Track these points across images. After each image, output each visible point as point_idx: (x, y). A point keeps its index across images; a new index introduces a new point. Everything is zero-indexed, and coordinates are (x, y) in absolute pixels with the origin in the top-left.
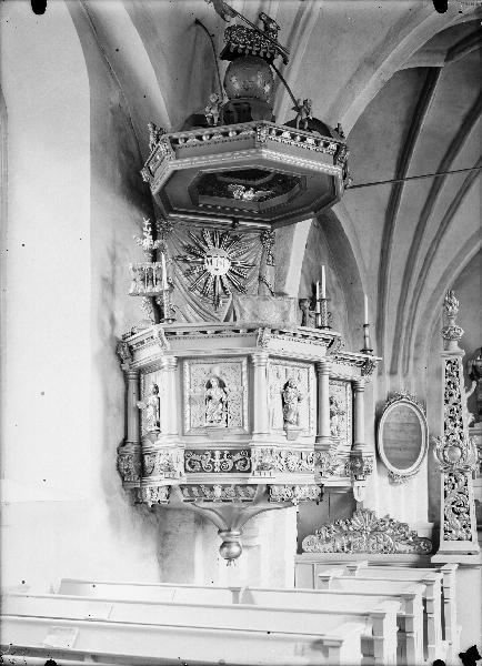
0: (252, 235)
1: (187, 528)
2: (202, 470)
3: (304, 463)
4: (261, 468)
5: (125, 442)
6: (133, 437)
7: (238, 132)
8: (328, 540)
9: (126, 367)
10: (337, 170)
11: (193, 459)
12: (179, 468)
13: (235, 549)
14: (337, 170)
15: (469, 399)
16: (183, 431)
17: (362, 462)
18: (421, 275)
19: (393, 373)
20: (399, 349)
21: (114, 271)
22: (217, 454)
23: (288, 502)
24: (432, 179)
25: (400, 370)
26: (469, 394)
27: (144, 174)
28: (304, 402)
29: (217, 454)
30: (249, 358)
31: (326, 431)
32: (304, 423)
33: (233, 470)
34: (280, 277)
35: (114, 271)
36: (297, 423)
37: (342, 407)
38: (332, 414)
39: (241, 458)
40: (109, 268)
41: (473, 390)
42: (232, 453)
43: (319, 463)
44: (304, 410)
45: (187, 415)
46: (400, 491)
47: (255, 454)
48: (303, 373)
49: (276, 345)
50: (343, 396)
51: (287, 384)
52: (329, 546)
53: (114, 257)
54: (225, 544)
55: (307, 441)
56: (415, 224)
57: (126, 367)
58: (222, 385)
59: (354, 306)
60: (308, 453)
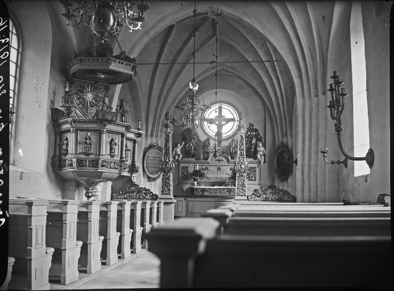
0: (102, 87)
1: (73, 188)
2: (82, 166)
3: (116, 166)
4: (103, 166)
5: (54, 156)
6: (57, 154)
7: (102, 60)
8: (122, 195)
9: (56, 130)
10: (132, 73)
11: (80, 163)
12: (75, 165)
13: (90, 194)
14: (132, 73)
15: (181, 148)
16: (77, 151)
17: (135, 167)
18: (165, 98)
19: (152, 136)
20: (154, 127)
21: (54, 97)
22: (88, 161)
23: (108, 179)
24: (169, 65)
25: (155, 134)
26: (181, 146)
27: (68, 67)
28: (117, 146)
29: (88, 161)
30: (100, 131)
31: (124, 156)
32: (116, 153)
33: (93, 167)
34: (111, 102)
35: (54, 97)
36: (114, 152)
37: (129, 148)
38: (126, 150)
39: (95, 163)
40: (53, 97)
41: (183, 145)
42: (93, 161)
43: (121, 166)
44: (117, 151)
45: (78, 148)
46: (152, 184)
47: (100, 162)
48: (117, 136)
49: (109, 127)
50: (130, 145)
51: (112, 140)
52: (122, 197)
53: (54, 93)
54: (87, 192)
55: (117, 158)
56: (164, 78)
57: (56, 130)
58: (90, 139)
59: (137, 109)
60: (117, 163)
